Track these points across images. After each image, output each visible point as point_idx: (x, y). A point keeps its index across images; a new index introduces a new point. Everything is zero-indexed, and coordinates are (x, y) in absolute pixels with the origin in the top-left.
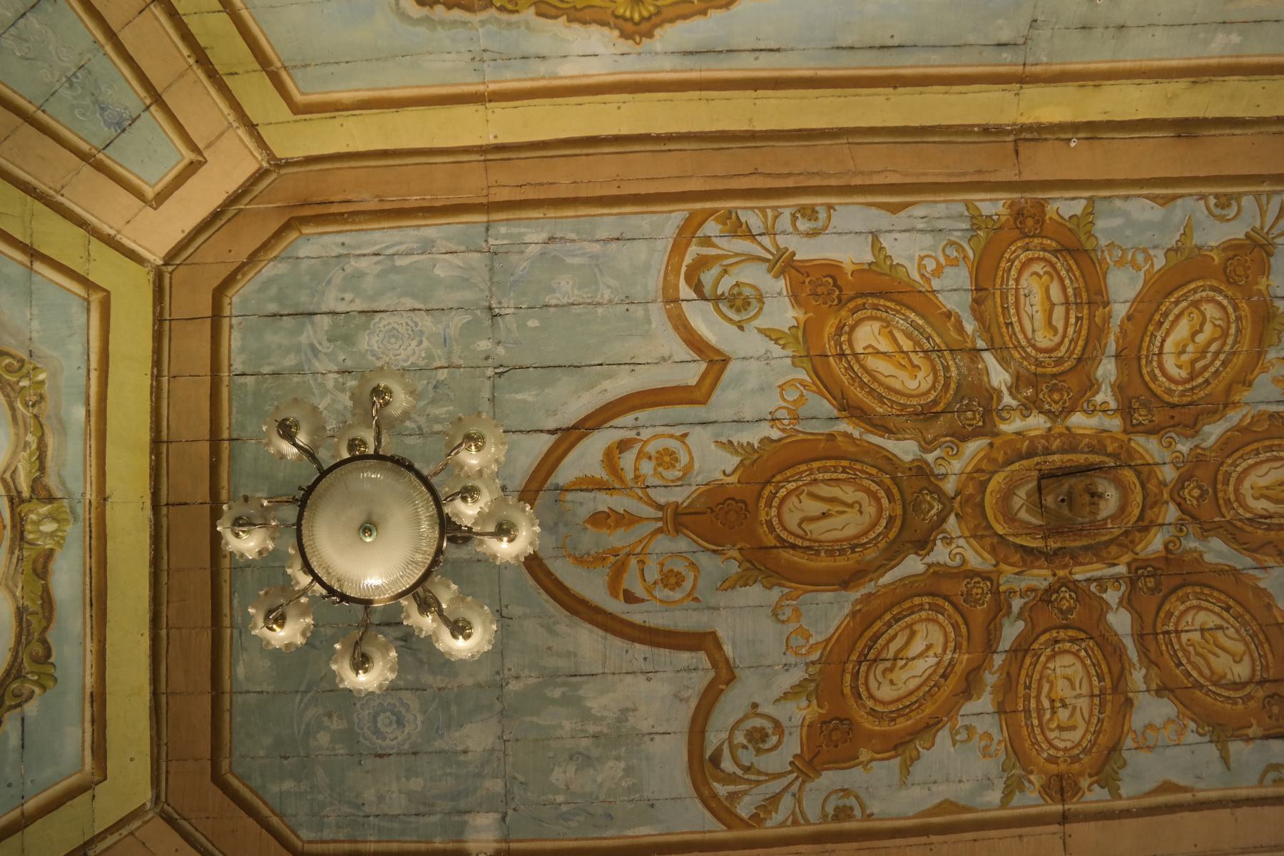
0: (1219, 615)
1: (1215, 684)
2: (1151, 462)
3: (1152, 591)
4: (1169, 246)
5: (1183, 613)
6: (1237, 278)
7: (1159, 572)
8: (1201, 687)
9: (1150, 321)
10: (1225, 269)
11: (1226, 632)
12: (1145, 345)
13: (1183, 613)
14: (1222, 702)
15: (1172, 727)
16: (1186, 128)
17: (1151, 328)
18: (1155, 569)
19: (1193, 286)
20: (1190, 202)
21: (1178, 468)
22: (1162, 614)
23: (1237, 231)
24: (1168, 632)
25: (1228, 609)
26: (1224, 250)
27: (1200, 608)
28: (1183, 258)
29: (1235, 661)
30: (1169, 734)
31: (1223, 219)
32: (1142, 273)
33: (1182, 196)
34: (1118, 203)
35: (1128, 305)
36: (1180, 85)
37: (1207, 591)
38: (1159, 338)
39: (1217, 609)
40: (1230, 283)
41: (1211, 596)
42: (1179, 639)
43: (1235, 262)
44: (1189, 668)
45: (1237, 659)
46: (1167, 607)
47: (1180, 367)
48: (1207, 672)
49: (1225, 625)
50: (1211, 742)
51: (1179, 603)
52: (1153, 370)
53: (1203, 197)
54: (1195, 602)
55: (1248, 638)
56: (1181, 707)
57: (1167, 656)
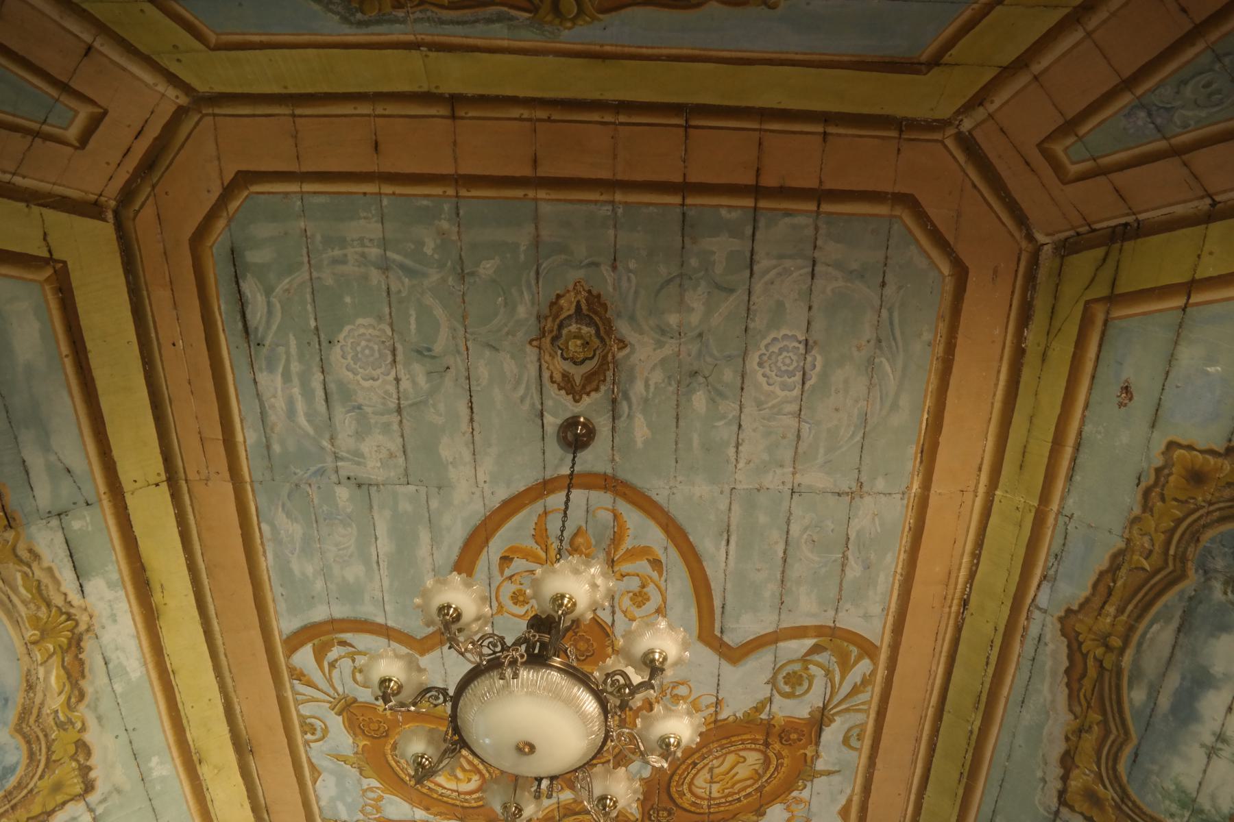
0: (699, 771)
1: (760, 777)
2: (557, 805)
3: (670, 814)
4: (358, 774)
5: (693, 794)
6: (382, 729)
7: (655, 806)
8: (763, 786)
9: (428, 796)
10: (376, 738)
11: (716, 765)
12: (450, 801)
13: (693, 794)
14: (778, 773)
15: (793, 807)
16: (242, 747)
17: (435, 796)
18: (652, 808)
19: (393, 763)
20: (313, 754)
21: (562, 788)
22: (693, 809)
23: (336, 723)
24: (709, 807)
25: (695, 764)
26: (355, 735)
27: (691, 784)
28: (366, 765)
29: (743, 762)
30: (799, 810)
31: (326, 731)
32: (385, 795)
33: (309, 759)
34: (323, 803)
35: (415, 809)
36: (205, 771)
37: (676, 778)
38: (444, 791)
39: (694, 772)
40: (387, 736)
41: (680, 775)
42: (715, 799)
43: (366, 729)
44: (744, 793)
45: (742, 760)
46: (686, 806)
47: (469, 780)
48: (749, 782)
49: (710, 766)
50: (812, 781)
51: (684, 798)
52: (474, 799)
53: (307, 743)
54: (685, 787)
55: (724, 751)
56: (778, 800)
57: (731, 808)
